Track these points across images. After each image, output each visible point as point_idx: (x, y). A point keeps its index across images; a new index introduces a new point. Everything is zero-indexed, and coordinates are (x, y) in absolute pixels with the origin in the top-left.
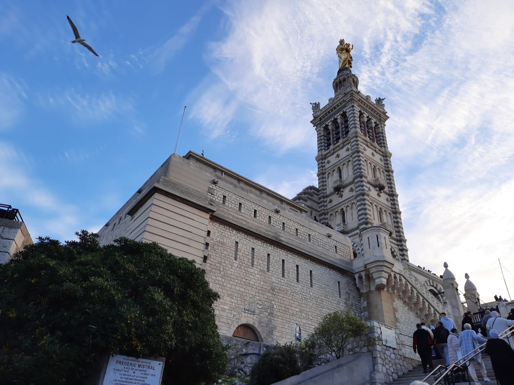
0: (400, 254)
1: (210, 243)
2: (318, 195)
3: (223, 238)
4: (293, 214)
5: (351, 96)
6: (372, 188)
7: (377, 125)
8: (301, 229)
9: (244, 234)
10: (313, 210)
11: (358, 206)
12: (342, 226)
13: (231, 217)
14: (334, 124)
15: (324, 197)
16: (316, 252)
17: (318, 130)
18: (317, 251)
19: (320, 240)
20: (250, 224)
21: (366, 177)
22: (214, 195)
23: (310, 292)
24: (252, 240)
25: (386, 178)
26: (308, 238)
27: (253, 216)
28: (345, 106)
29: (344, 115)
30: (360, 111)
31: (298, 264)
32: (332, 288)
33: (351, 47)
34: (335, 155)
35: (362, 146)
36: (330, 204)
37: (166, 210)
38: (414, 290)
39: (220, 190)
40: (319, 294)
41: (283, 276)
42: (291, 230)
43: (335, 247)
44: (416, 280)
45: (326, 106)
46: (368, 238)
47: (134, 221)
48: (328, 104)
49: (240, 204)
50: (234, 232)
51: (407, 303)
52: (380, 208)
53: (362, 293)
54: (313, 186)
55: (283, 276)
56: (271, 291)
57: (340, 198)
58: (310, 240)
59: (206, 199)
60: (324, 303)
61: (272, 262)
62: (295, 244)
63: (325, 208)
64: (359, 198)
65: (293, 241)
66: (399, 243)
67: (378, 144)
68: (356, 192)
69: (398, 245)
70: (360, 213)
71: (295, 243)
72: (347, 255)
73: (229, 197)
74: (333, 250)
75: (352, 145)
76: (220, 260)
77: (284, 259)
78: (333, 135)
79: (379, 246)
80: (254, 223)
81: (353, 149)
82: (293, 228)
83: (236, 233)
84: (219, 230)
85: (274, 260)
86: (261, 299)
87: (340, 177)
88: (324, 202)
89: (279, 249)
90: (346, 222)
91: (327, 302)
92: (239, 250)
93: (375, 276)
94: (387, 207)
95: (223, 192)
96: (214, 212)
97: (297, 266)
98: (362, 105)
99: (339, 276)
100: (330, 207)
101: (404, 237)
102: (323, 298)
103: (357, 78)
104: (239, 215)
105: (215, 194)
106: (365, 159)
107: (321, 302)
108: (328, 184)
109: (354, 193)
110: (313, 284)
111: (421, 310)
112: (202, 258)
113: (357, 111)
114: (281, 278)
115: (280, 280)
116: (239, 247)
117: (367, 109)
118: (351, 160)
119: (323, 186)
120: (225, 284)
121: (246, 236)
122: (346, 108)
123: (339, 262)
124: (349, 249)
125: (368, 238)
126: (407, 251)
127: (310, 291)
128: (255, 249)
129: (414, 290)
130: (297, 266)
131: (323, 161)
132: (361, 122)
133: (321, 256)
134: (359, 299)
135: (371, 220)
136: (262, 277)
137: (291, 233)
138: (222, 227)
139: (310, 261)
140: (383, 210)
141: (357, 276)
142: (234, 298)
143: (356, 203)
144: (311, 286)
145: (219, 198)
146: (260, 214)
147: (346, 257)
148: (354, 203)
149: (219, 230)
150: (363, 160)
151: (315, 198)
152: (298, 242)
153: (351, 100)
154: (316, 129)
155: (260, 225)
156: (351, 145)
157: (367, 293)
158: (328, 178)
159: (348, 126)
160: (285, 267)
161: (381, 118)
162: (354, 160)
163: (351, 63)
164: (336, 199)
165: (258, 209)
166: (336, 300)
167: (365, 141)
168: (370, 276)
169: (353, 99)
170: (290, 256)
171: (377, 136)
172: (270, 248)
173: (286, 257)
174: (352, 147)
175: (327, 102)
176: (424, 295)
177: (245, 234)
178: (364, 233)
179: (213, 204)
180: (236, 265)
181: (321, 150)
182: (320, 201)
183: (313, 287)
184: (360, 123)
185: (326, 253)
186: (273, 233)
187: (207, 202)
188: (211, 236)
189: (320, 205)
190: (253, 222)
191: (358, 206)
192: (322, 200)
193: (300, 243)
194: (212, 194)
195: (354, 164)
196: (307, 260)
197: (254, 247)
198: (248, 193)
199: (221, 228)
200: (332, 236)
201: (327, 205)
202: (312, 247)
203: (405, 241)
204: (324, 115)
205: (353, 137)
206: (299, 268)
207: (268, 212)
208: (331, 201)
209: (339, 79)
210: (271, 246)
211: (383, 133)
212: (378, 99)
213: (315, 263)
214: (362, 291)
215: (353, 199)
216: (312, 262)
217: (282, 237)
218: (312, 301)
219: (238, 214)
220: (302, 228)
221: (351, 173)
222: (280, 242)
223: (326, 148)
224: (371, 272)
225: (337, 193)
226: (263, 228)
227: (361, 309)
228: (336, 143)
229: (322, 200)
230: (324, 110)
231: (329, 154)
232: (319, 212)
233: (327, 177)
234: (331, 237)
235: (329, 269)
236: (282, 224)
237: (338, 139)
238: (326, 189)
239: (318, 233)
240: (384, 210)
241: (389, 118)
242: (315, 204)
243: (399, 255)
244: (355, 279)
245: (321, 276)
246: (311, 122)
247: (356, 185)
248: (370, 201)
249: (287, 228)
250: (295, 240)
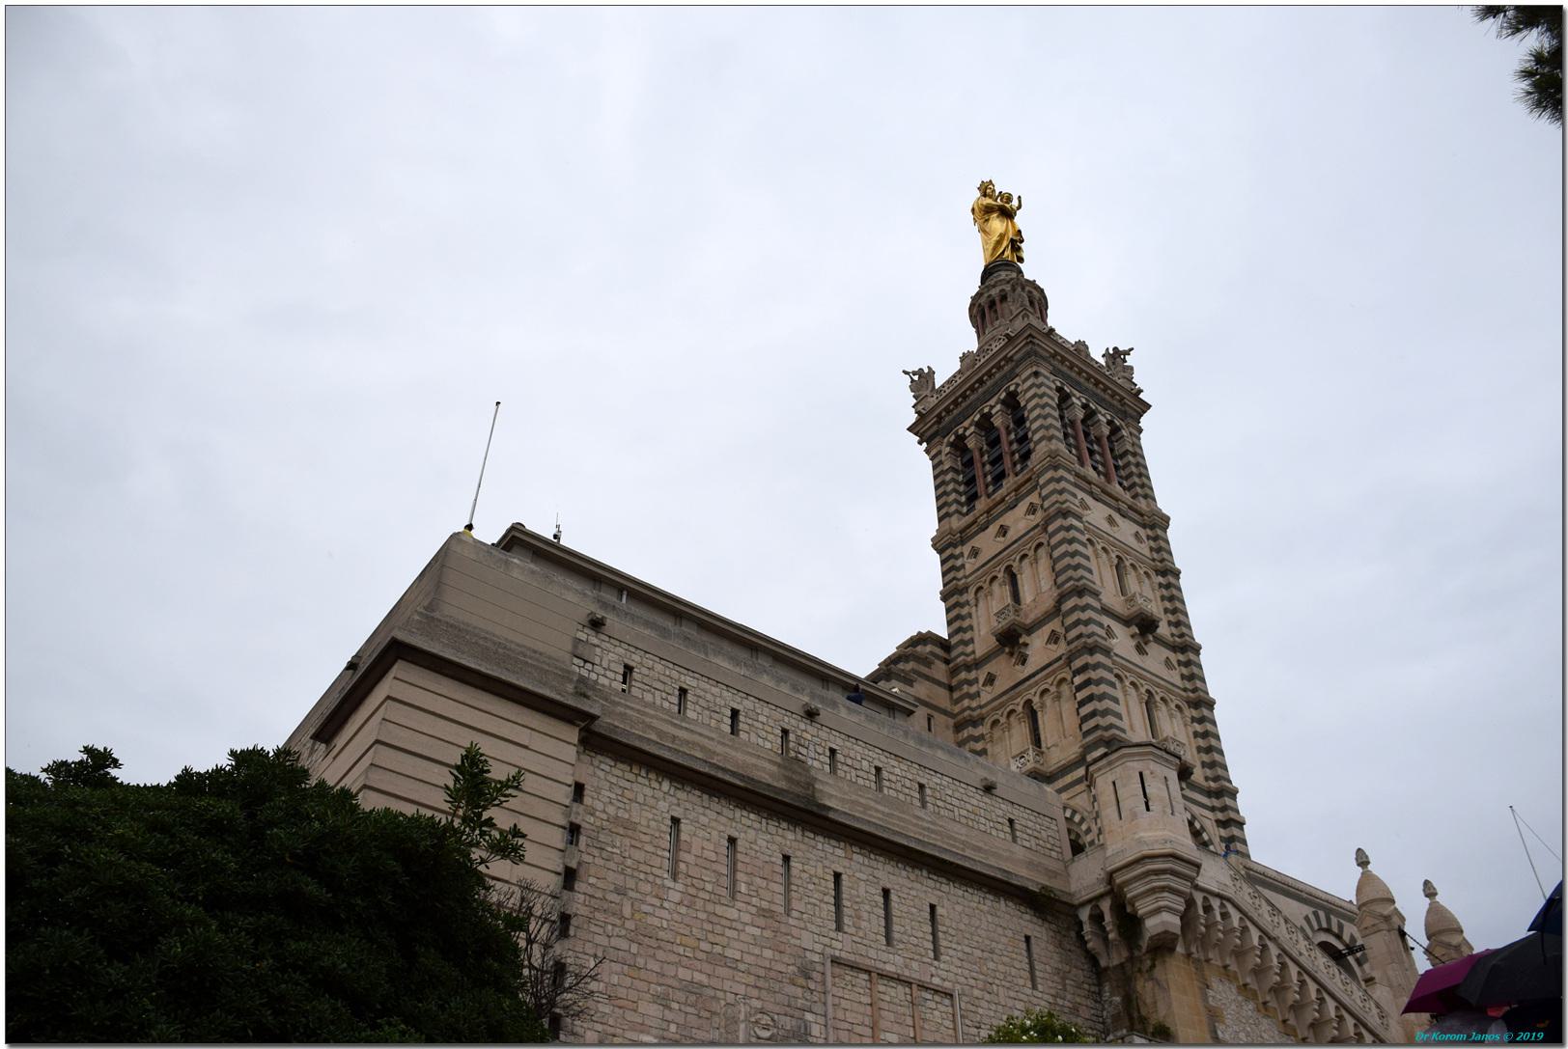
0: (1221, 837)
1: (584, 825)
3: (628, 808)
4: (863, 718)
5: (1027, 343)
6: (1117, 628)
7: (1115, 430)
8: (894, 769)
9: (698, 793)
10: (935, 714)
11: (1079, 688)
12: (1031, 758)
13: (654, 737)
14: (983, 434)
15: (968, 668)
16: (948, 844)
17: (933, 453)
18: (950, 837)
19: (956, 802)
20: (719, 758)
21: (1096, 594)
22: (593, 664)
23: (932, 976)
24: (726, 811)
25: (1158, 594)
26: (917, 795)
27: (728, 729)
28: (1012, 375)
29: (1012, 403)
30: (1059, 390)
31: (888, 886)
32: (1005, 959)
33: (1015, 203)
34: (993, 529)
35: (1075, 496)
36: (988, 688)
37: (433, 717)
38: (1271, 945)
39: (611, 648)
40: (962, 980)
41: (839, 928)
42: (860, 773)
43: (1008, 824)
44: (1275, 910)
45: (954, 376)
46: (1114, 783)
47: (334, 758)
48: (959, 372)
49: (683, 692)
50: (666, 786)
51: (1251, 989)
52: (1148, 691)
53: (1107, 969)
54: (929, 632)
55: (839, 928)
56: (801, 981)
57: (1019, 667)
58: (924, 805)
59: (566, 675)
60: (980, 1011)
61: (799, 882)
62: (873, 820)
63: (974, 704)
64: (1078, 663)
65: (866, 808)
66: (1216, 803)
67: (1124, 488)
68: (1069, 643)
69: (1213, 809)
70: (1086, 710)
71: (875, 814)
72: (1049, 846)
73: (645, 671)
74: (1002, 835)
75: (1044, 492)
76: (620, 880)
77: (839, 870)
78: (984, 465)
79: (1148, 809)
80: (734, 753)
81: (1049, 508)
83: (673, 789)
84: (614, 780)
85: (805, 876)
86: (769, 1007)
87: (1016, 596)
88: (970, 683)
89: (820, 838)
90: (1043, 745)
91: (993, 1007)
92: (683, 846)
93: (1143, 907)
94: (1170, 687)
95: (621, 651)
96: (593, 718)
97: (886, 893)
98: (1065, 369)
99: (1027, 917)
100: (989, 697)
101: (1230, 782)
102: (976, 993)
103: (1042, 290)
104: (681, 728)
105: (597, 660)
106: (1087, 536)
107: (973, 1008)
108: (979, 624)
109: (1062, 648)
110: (942, 950)
111: (1297, 1008)
112: (559, 874)
114: (833, 934)
115: (826, 941)
116: (684, 837)
117: (1082, 380)
118: (1046, 543)
119: (959, 630)
120: (641, 962)
121: (706, 797)
122: (1017, 380)
123: (1023, 872)
125: (1114, 783)
126: (1240, 824)
127: (934, 972)
128: (739, 842)
129: (1269, 943)
130: (886, 893)
131: (957, 551)
132: (1068, 424)
133: (962, 855)
134: (1096, 989)
135: (1124, 731)
136: (768, 933)
137: (860, 781)
138: (623, 771)
139: (929, 873)
140: (1158, 698)
141: (1084, 915)
142: (675, 1006)
143: (1069, 679)
144: (936, 958)
145: (608, 673)
147: (1047, 852)
148: (1063, 680)
149: (614, 780)
150: (1083, 539)
152: (887, 810)
153: (1028, 355)
154: (927, 451)
155: (754, 761)
156: (1040, 494)
157: (1122, 965)
158: (976, 606)
159: (1026, 435)
160: (844, 896)
161: (1127, 409)
162: (1053, 541)
163: (1019, 249)
164: (1006, 672)
165: (744, 705)
166: (1022, 997)
167: (1084, 479)
168: (1129, 909)
169: (1036, 354)
170: (860, 859)
171: (1120, 463)
172: (790, 836)
173: (846, 863)
174: (1044, 499)
175: (957, 366)
176: (1302, 960)
177: (703, 792)
178: (1100, 769)
179: (590, 693)
180: (675, 897)
181: (948, 515)
182: (954, 682)
183: (942, 958)
184: (1064, 426)
185: (980, 844)
186: (798, 783)
187: (570, 688)
188: (587, 800)
190: (728, 750)
191: (1079, 688)
192: (963, 675)
193: (888, 815)
194: (586, 661)
195: (1056, 554)
196: (917, 872)
197: (735, 834)
198: (706, 654)
199: (620, 774)
200: (998, 786)
201: (978, 694)
202: (932, 827)
203: (1233, 793)
204: (950, 405)
205: (1046, 470)
206: (893, 897)
207: (777, 714)
208: (990, 680)
209: (986, 295)
210: (791, 828)
211: (1138, 454)
212: (1111, 352)
213: (944, 881)
214: (1103, 963)
215: (1061, 668)
216: (935, 878)
218: (939, 1006)
219: (675, 725)
220: (895, 763)
221: (1046, 582)
222: (824, 813)
223: (965, 509)
224: (1128, 896)
225: (1007, 650)
226: (764, 769)
227: (1103, 1023)
228: (994, 492)
230: (947, 392)
231: (974, 528)
233: (973, 602)
234: (994, 791)
235: (991, 897)
236: (828, 753)
237: (999, 478)
238: (972, 640)
239: (950, 780)
240: (1162, 699)
241: (1148, 406)
243: (1216, 840)
244: (1080, 924)
245: (966, 920)
247: (1069, 621)
248: (1116, 671)
249: (846, 768)
250: (872, 804)
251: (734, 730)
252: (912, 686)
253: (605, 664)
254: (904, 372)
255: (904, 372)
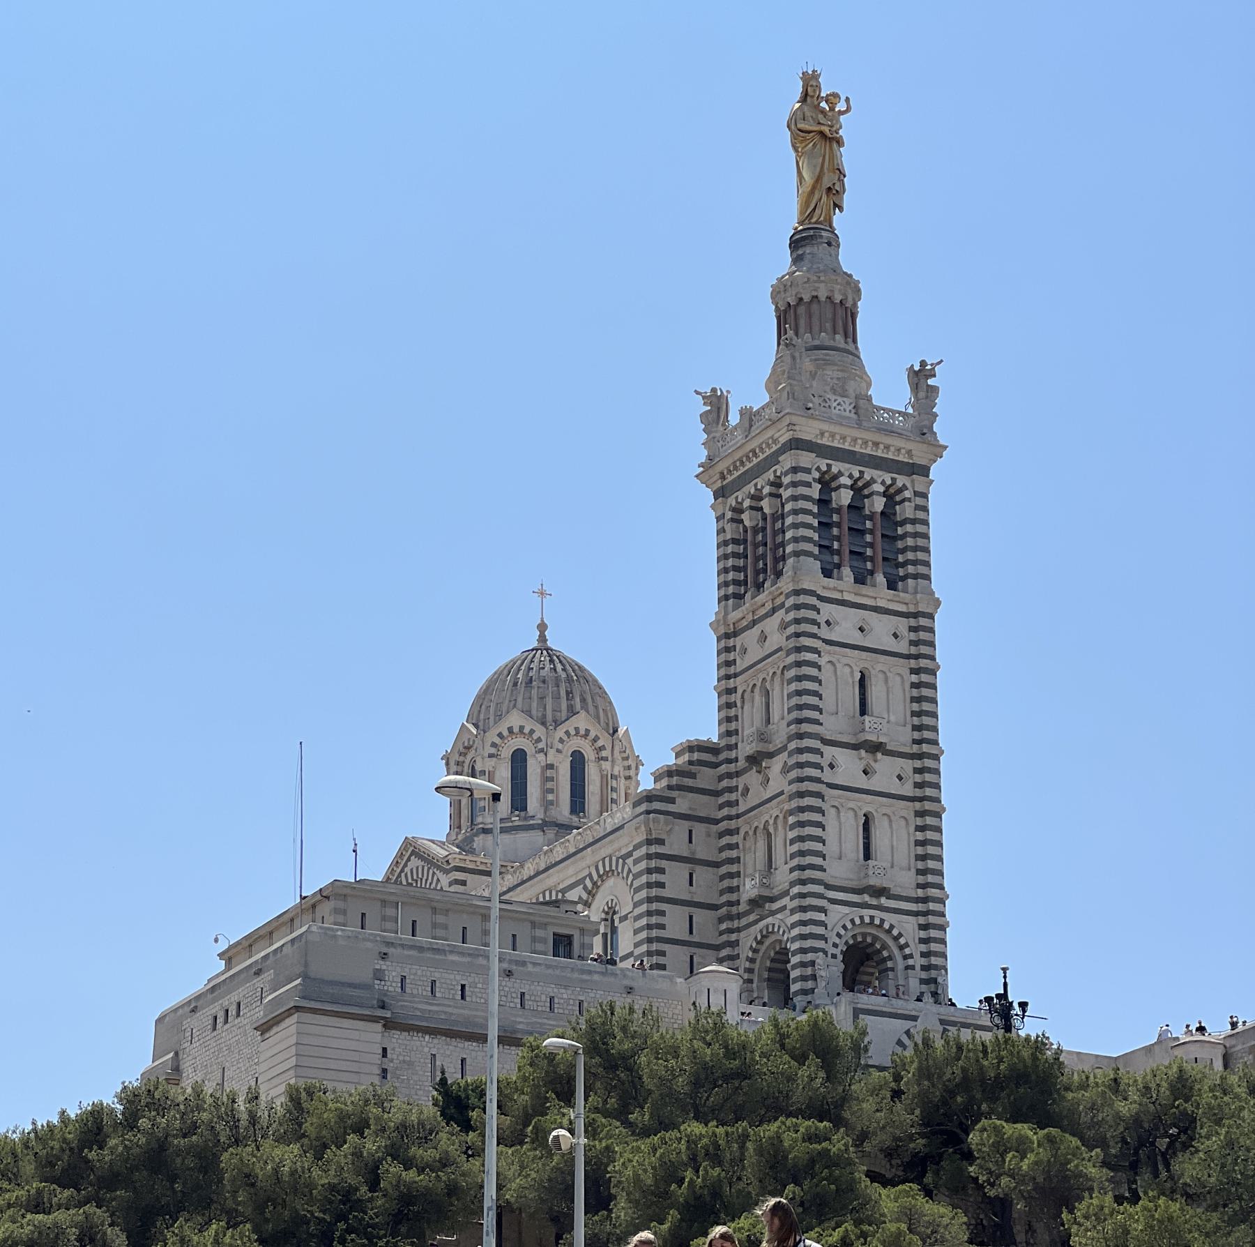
2: (715, 766)
6: (841, 756)
7: (891, 496)
13: (419, 1014)
15: (729, 776)
33: (841, 106)
42: (539, 1004)
66: (921, 907)
69: (916, 914)
82: (543, 997)
88: (730, 790)
89: (513, 1048)
108: (743, 727)
113: (808, 485)
124: (679, 1007)
146: (471, 989)
151: (706, 778)
158: (742, 708)
189: (721, 800)
192: (725, 783)
198: (445, 955)
208: (746, 790)
217: (520, 1023)
220: (563, 991)
229: (725, 783)
232: (717, 822)
241: (946, 447)
242: (706, 798)
246: (697, 476)
249: (530, 1003)
250: (545, 1021)
251: (463, 997)
252: (674, 803)
253: (391, 979)
254: (696, 391)
255: (696, 391)
